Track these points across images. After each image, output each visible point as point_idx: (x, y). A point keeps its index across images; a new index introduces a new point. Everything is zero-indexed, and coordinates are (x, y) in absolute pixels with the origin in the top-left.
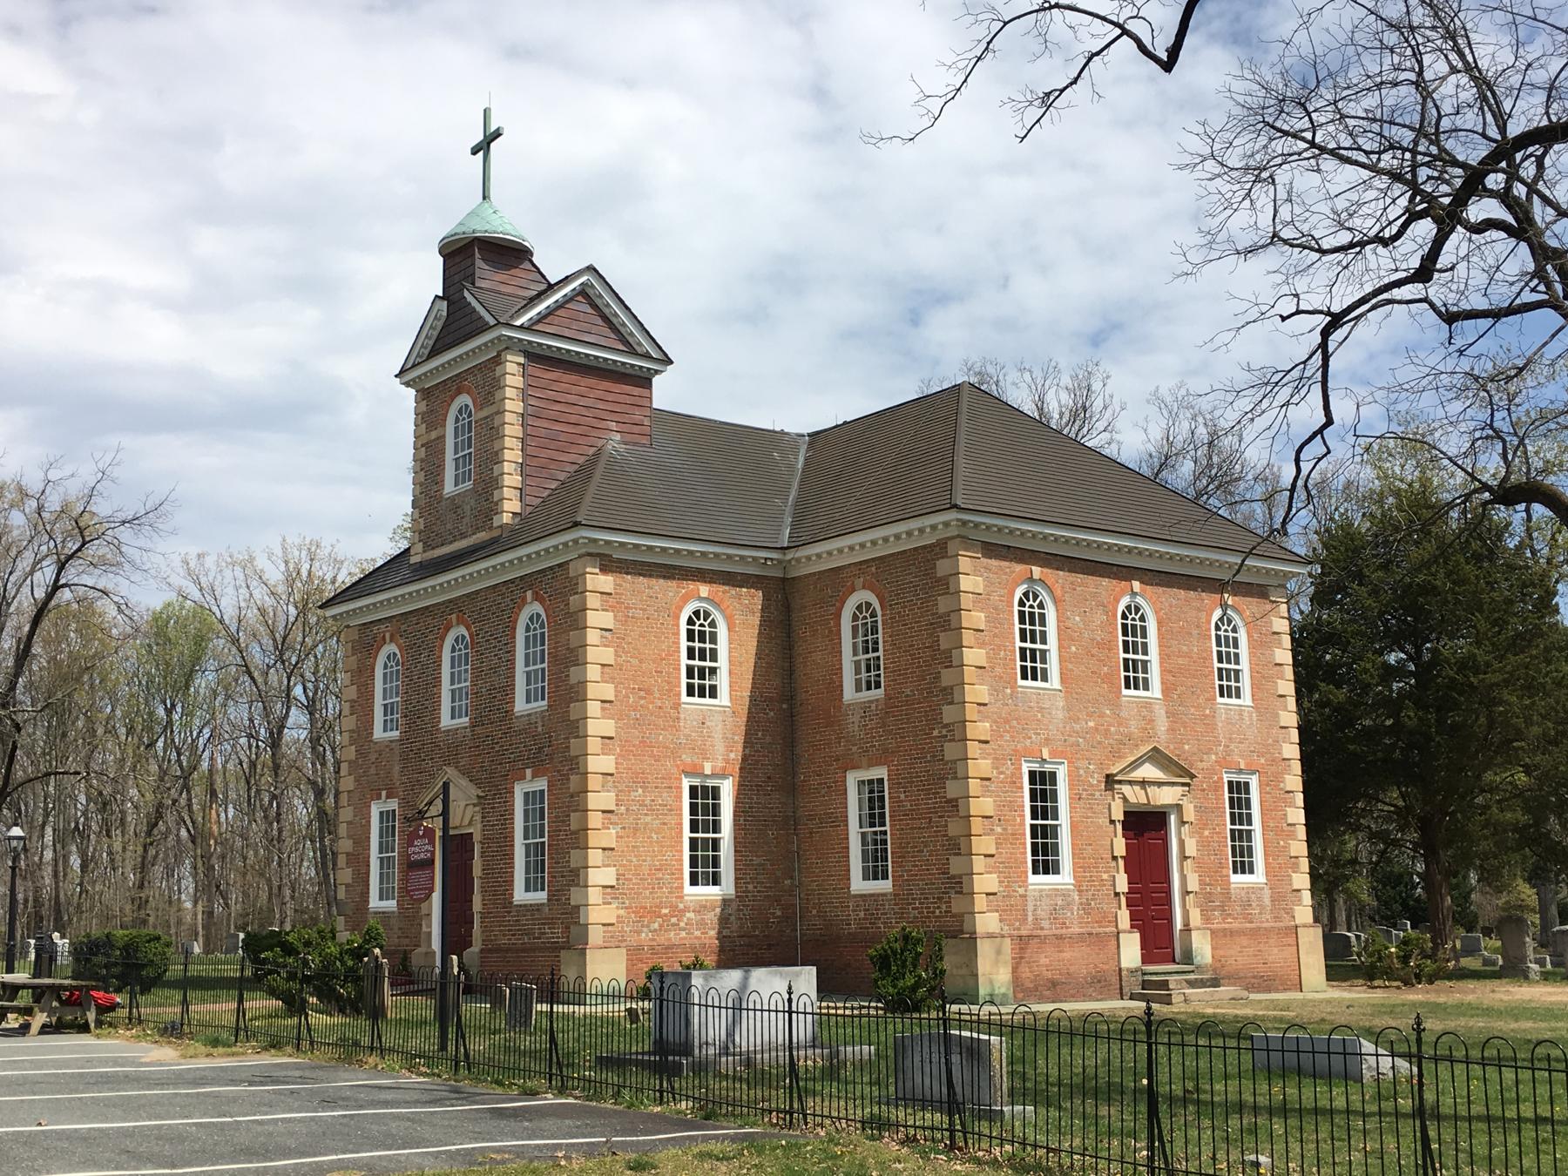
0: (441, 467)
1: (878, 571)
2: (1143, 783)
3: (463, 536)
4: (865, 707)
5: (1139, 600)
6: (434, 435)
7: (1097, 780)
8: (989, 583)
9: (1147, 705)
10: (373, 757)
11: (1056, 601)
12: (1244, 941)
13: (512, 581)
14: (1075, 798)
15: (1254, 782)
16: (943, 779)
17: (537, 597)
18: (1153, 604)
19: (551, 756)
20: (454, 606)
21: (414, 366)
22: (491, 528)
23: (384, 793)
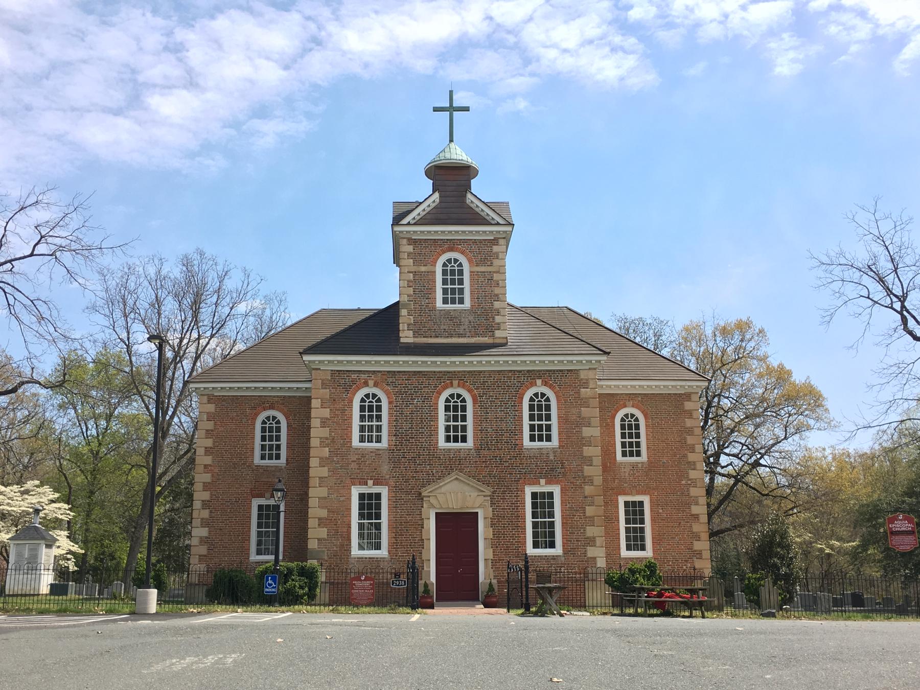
0: (433, 289)
1: (643, 400)
3: (460, 336)
4: (634, 466)
6: (423, 269)
10: (354, 458)
13: (520, 371)
16: (688, 505)
17: (545, 384)
19: (564, 475)
20: (462, 378)
21: (409, 224)
22: (493, 336)
23: (370, 482)
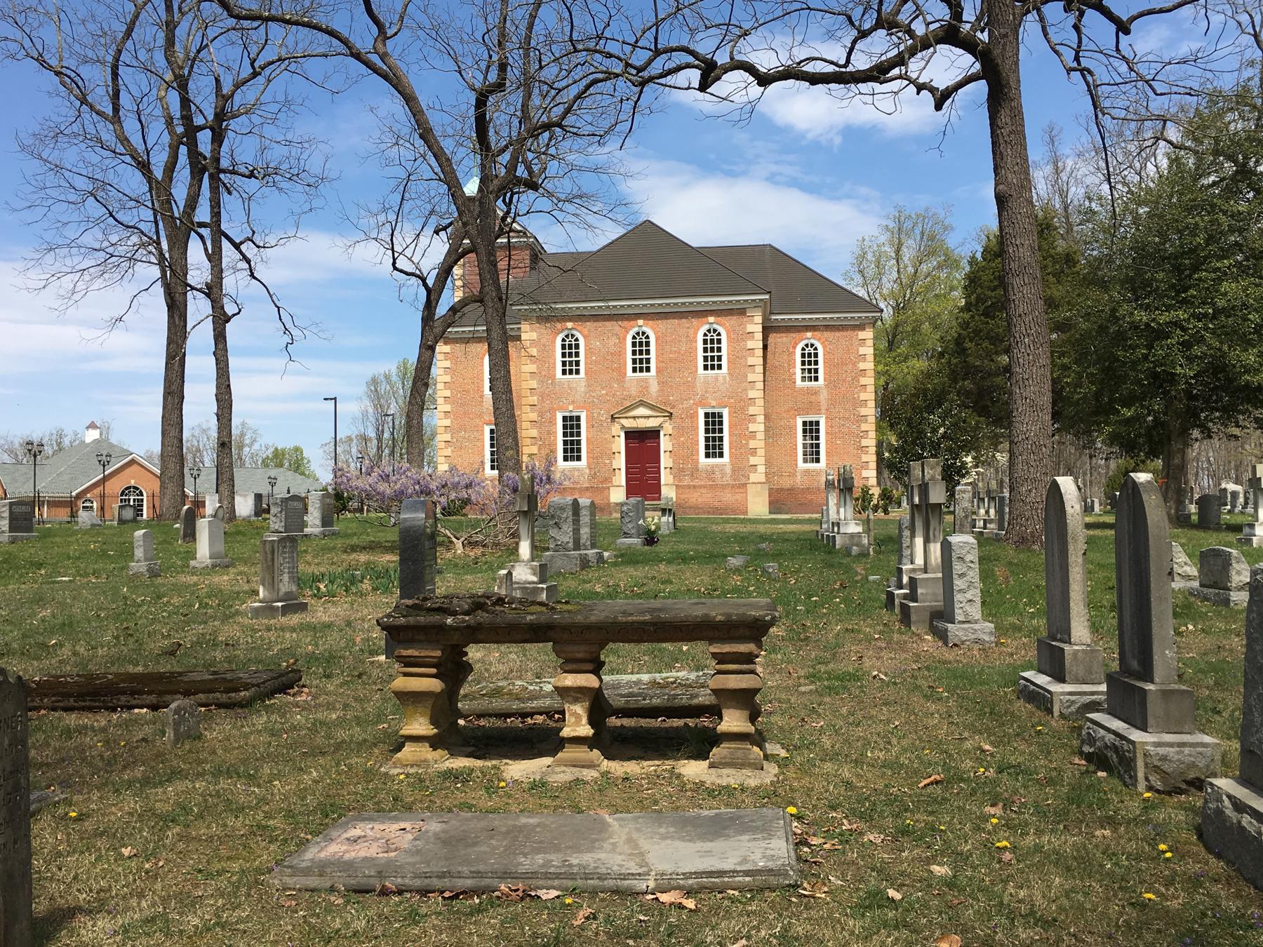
2: (634, 418)
5: (644, 329)
7: (605, 417)
8: (540, 334)
9: (646, 380)
11: (585, 337)
12: (704, 491)
14: (590, 426)
15: (726, 413)
18: (652, 328)
